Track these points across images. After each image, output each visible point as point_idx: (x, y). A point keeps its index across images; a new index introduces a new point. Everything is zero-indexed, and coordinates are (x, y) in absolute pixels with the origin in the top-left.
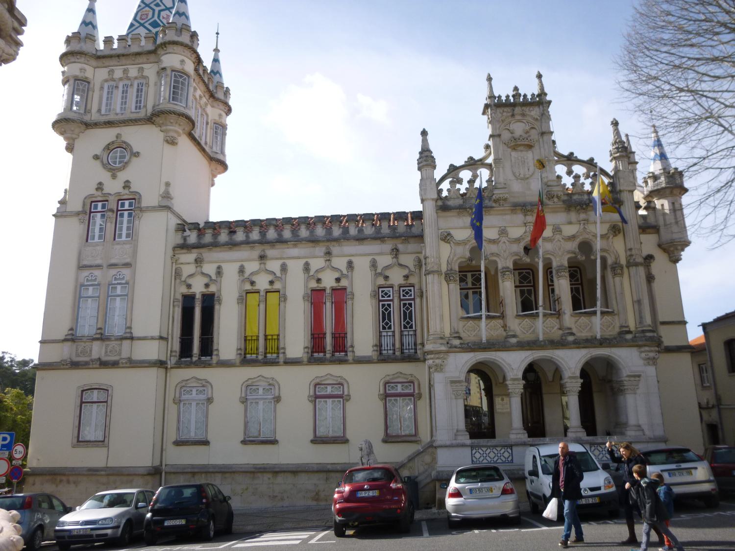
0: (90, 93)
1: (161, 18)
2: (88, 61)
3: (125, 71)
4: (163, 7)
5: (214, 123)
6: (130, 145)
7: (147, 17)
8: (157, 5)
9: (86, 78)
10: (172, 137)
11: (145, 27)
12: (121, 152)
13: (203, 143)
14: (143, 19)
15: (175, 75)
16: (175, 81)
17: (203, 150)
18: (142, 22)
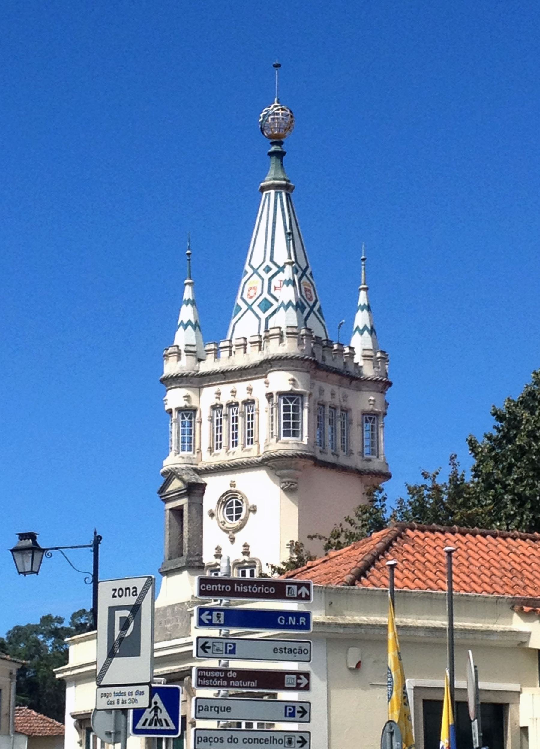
0: (198, 425)
1: (273, 291)
2: (191, 383)
3: (234, 393)
4: (275, 269)
5: (363, 414)
6: (245, 497)
7: (255, 294)
8: (268, 269)
9: (191, 407)
10: (289, 482)
11: (253, 311)
12: (238, 503)
13: (343, 460)
14: (251, 297)
15: (285, 402)
16: (286, 409)
17: (344, 469)
18: (250, 302)
